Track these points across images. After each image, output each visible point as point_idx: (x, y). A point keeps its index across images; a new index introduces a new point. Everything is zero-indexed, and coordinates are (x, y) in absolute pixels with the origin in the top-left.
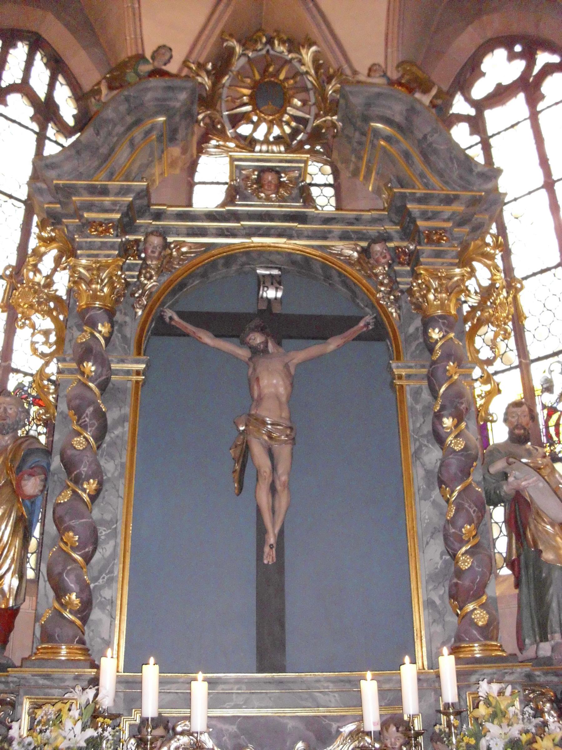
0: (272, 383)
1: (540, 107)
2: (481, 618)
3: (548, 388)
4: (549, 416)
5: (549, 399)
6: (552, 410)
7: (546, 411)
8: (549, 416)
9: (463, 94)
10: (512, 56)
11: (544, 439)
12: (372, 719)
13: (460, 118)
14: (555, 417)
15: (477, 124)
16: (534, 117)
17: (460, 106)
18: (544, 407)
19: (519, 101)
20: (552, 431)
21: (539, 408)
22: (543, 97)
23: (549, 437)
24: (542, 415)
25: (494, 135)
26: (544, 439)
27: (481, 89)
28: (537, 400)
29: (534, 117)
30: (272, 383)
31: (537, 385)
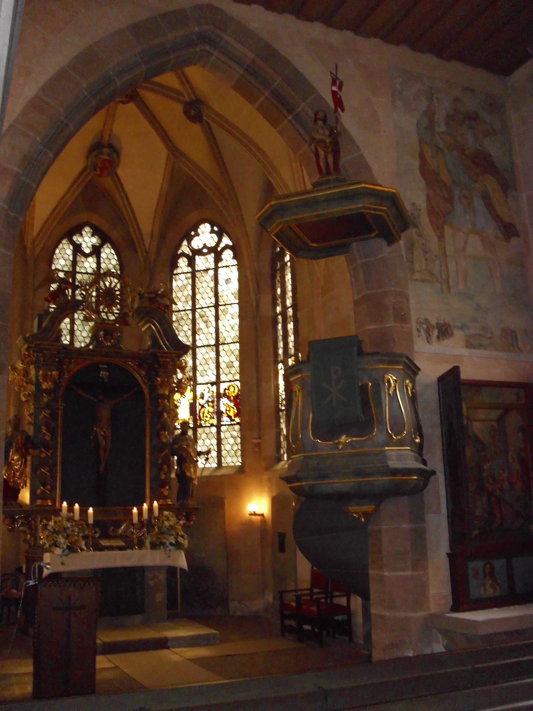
0: (105, 413)
1: (220, 265)
2: (166, 493)
3: (202, 398)
4: (201, 409)
5: (202, 402)
6: (203, 407)
7: (200, 407)
8: (201, 409)
9: (187, 242)
10: (212, 232)
11: (198, 418)
12: (135, 519)
13: (183, 254)
14: (203, 410)
15: (191, 263)
16: (216, 269)
17: (185, 248)
18: (200, 404)
19: (211, 257)
20: (201, 415)
21: (197, 405)
22: (221, 260)
23: (200, 417)
24: (198, 407)
25: (198, 271)
26: (198, 418)
27: (197, 243)
28: (197, 401)
29: (216, 269)
30: (105, 413)
31: (198, 395)
